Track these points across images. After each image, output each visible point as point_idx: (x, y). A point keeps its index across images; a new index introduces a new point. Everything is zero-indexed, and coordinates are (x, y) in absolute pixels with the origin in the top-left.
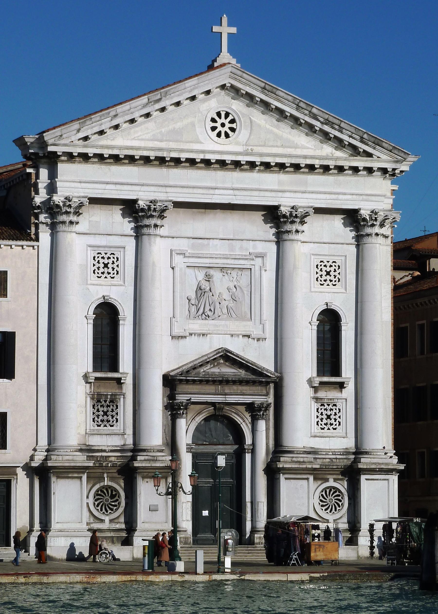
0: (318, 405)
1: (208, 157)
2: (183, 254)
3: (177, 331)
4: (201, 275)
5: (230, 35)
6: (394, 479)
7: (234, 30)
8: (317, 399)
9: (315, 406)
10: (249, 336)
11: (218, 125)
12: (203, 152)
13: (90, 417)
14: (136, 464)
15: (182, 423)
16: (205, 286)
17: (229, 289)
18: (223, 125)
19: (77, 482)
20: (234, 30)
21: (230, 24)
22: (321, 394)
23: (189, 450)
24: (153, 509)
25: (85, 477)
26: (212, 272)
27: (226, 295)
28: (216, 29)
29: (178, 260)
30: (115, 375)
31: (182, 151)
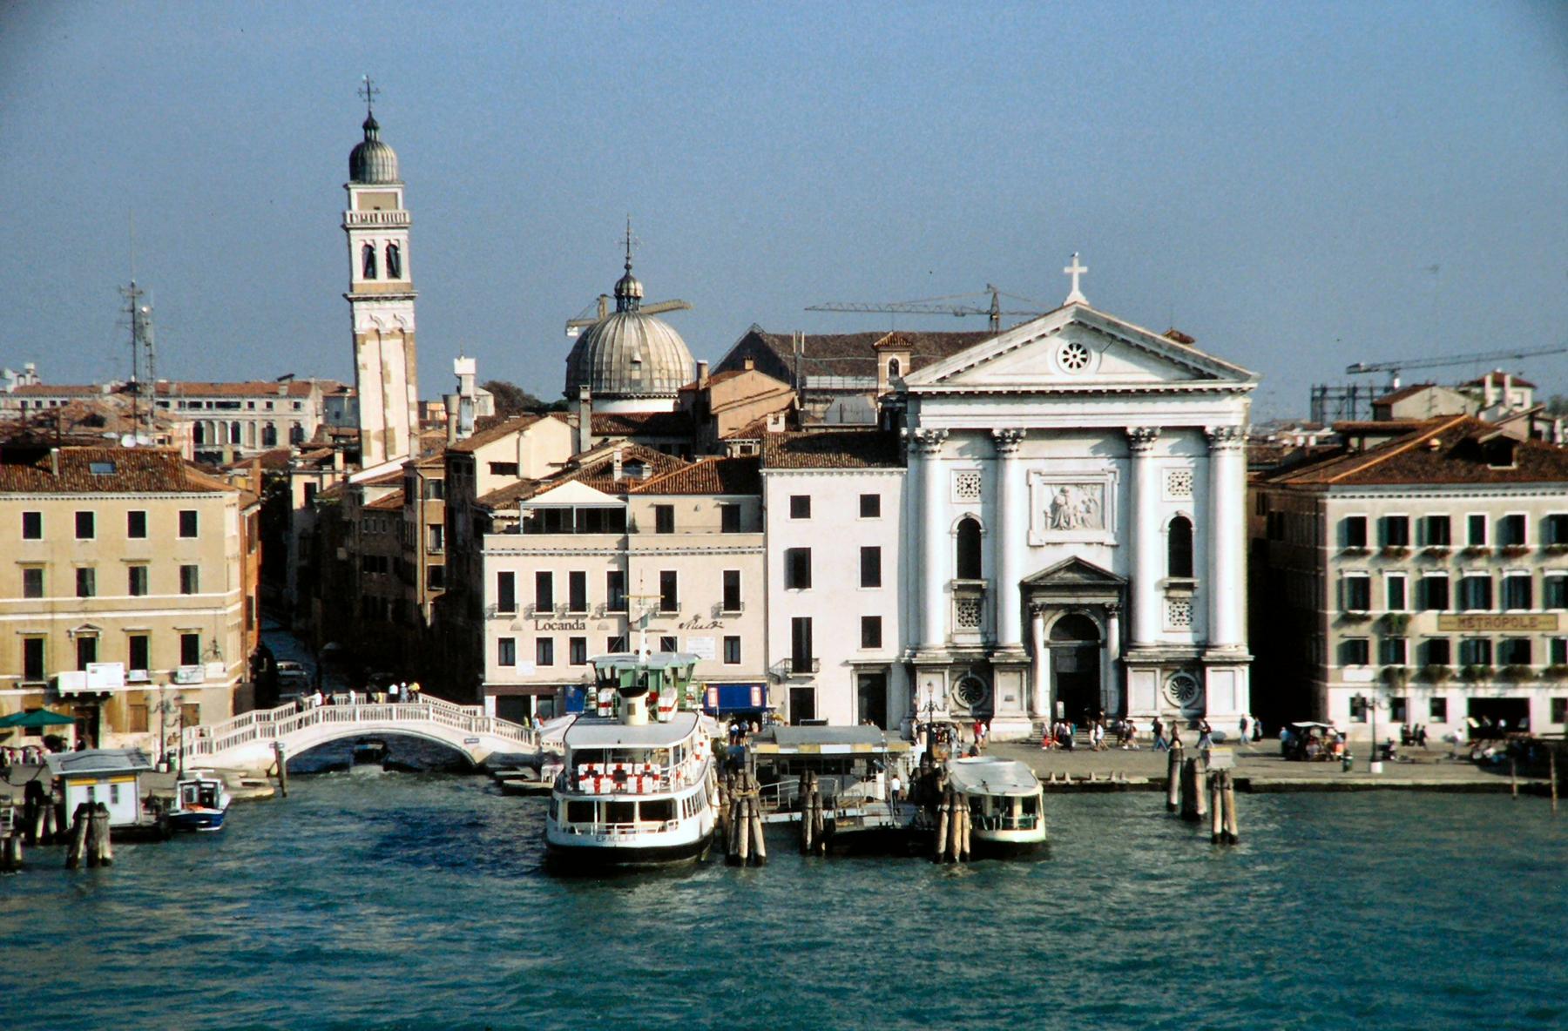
0: (1171, 603)
1: (1056, 388)
2: (1040, 474)
3: (1034, 542)
4: (1057, 490)
5: (1081, 275)
6: (1246, 668)
7: (1084, 269)
8: (1169, 598)
9: (1167, 604)
10: (1102, 544)
11: (1070, 356)
12: (1051, 384)
13: (955, 618)
14: (992, 660)
15: (1039, 623)
16: (1061, 500)
17: (1083, 502)
18: (1075, 356)
19: (940, 676)
20: (1084, 269)
21: (1081, 265)
22: (1173, 593)
23: (1047, 644)
24: (1008, 699)
25: (947, 672)
26: (1067, 488)
27: (1082, 508)
28: (1067, 270)
29: (1034, 479)
30: (977, 582)
31: (1031, 385)
